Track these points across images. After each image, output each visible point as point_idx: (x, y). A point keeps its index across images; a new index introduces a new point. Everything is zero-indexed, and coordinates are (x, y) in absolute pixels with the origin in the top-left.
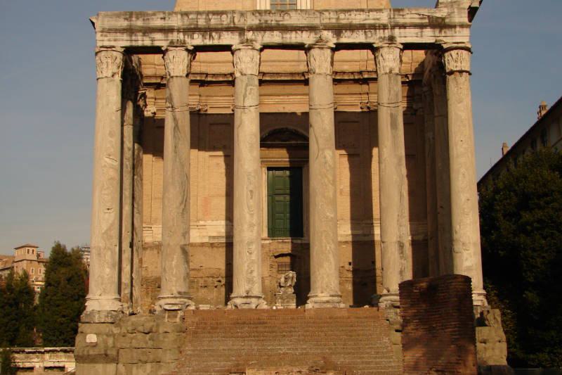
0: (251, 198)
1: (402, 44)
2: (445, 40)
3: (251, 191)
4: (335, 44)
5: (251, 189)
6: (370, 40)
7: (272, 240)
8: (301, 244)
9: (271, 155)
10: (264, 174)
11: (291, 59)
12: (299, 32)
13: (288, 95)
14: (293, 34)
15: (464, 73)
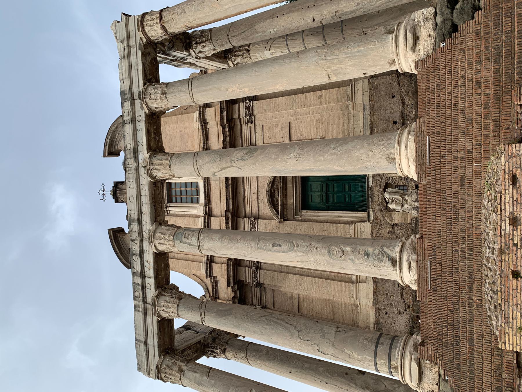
0: (280, 246)
1: (145, 84)
2: (138, 40)
3: (273, 246)
4: (148, 153)
5: (271, 245)
6: (143, 115)
7: (369, 208)
8: (373, 177)
9: (291, 206)
10: (308, 213)
11: (218, 187)
12: (142, 187)
13: (244, 190)
14: (143, 193)
15: (162, 13)
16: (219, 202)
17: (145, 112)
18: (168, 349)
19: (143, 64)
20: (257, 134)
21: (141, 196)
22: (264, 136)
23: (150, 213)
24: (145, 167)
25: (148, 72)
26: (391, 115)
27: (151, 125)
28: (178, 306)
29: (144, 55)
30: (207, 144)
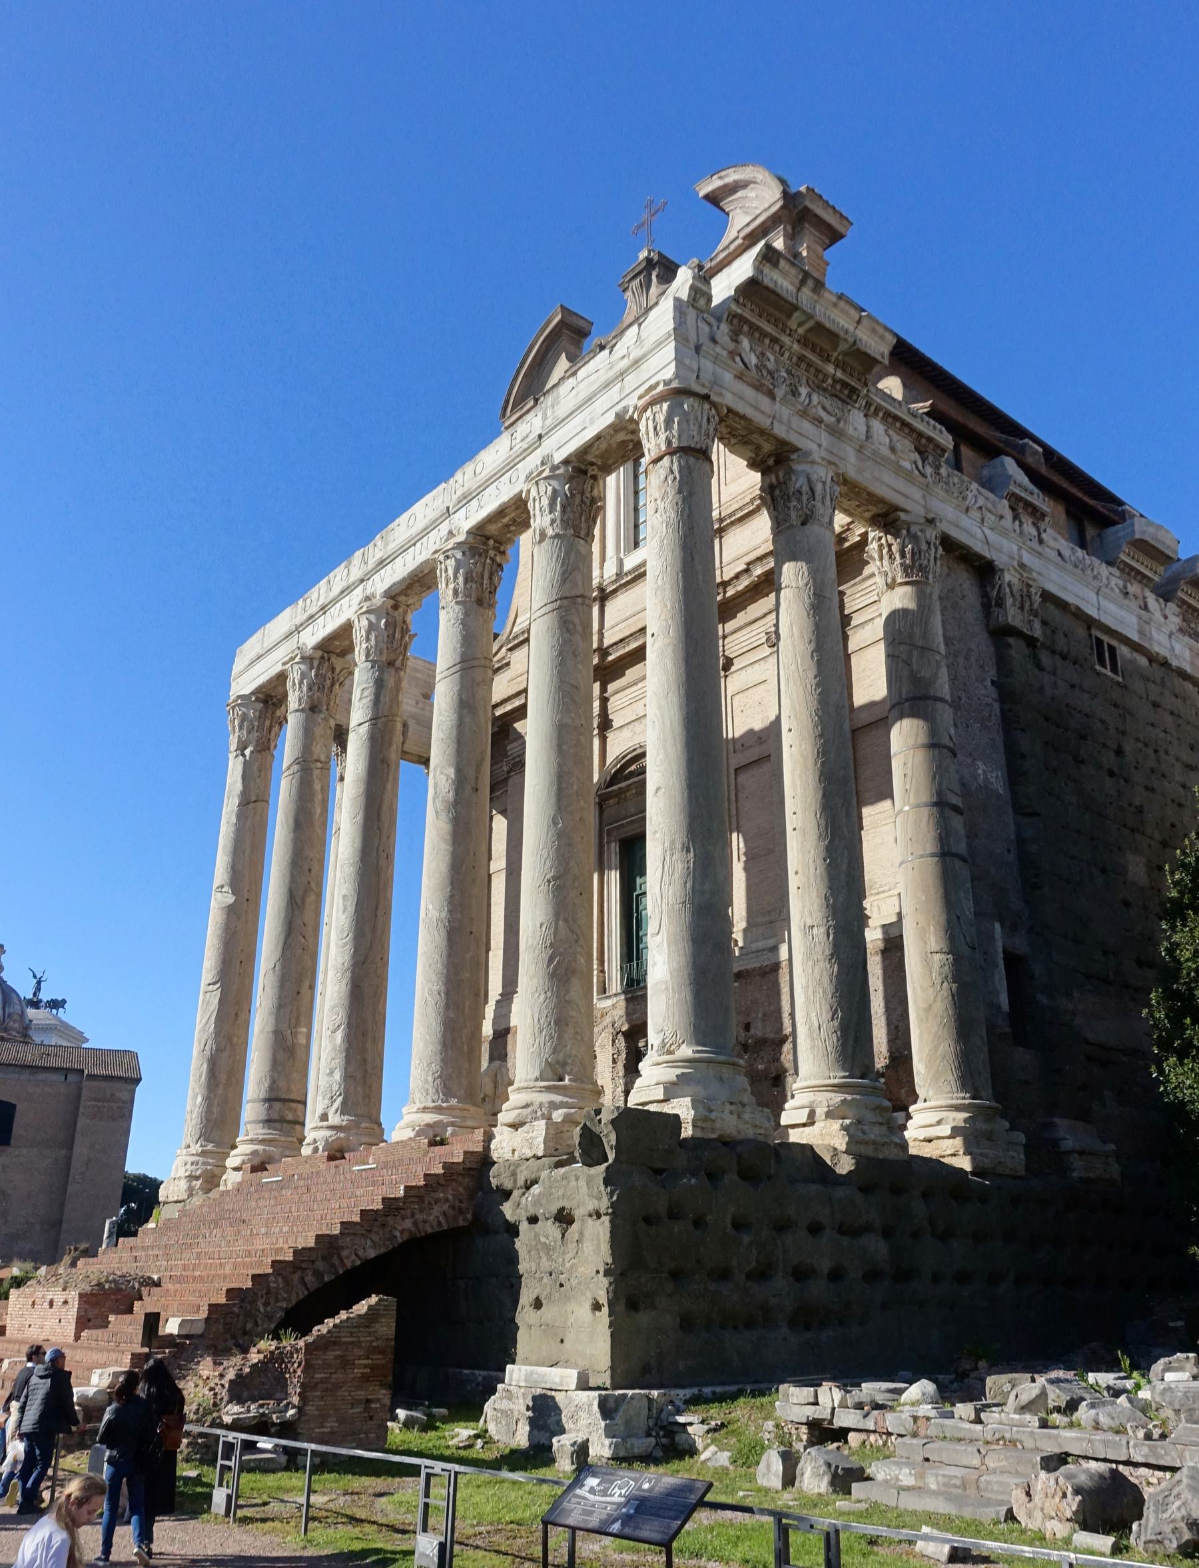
1: (566, 462)
4: (468, 532)
16: (630, 613)
17: (521, 492)
18: (271, 697)
19: (598, 437)
20: (749, 669)
21: (414, 545)
22: (746, 693)
23: (395, 584)
24: (451, 534)
25: (595, 451)
26: (760, 1015)
27: (517, 508)
28: (297, 711)
29: (615, 428)
30: (732, 523)
